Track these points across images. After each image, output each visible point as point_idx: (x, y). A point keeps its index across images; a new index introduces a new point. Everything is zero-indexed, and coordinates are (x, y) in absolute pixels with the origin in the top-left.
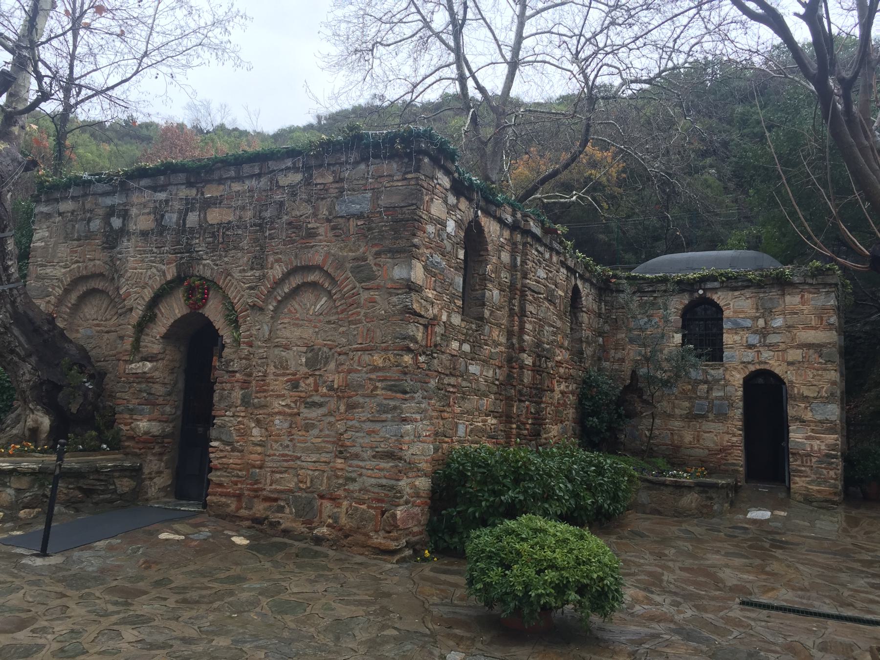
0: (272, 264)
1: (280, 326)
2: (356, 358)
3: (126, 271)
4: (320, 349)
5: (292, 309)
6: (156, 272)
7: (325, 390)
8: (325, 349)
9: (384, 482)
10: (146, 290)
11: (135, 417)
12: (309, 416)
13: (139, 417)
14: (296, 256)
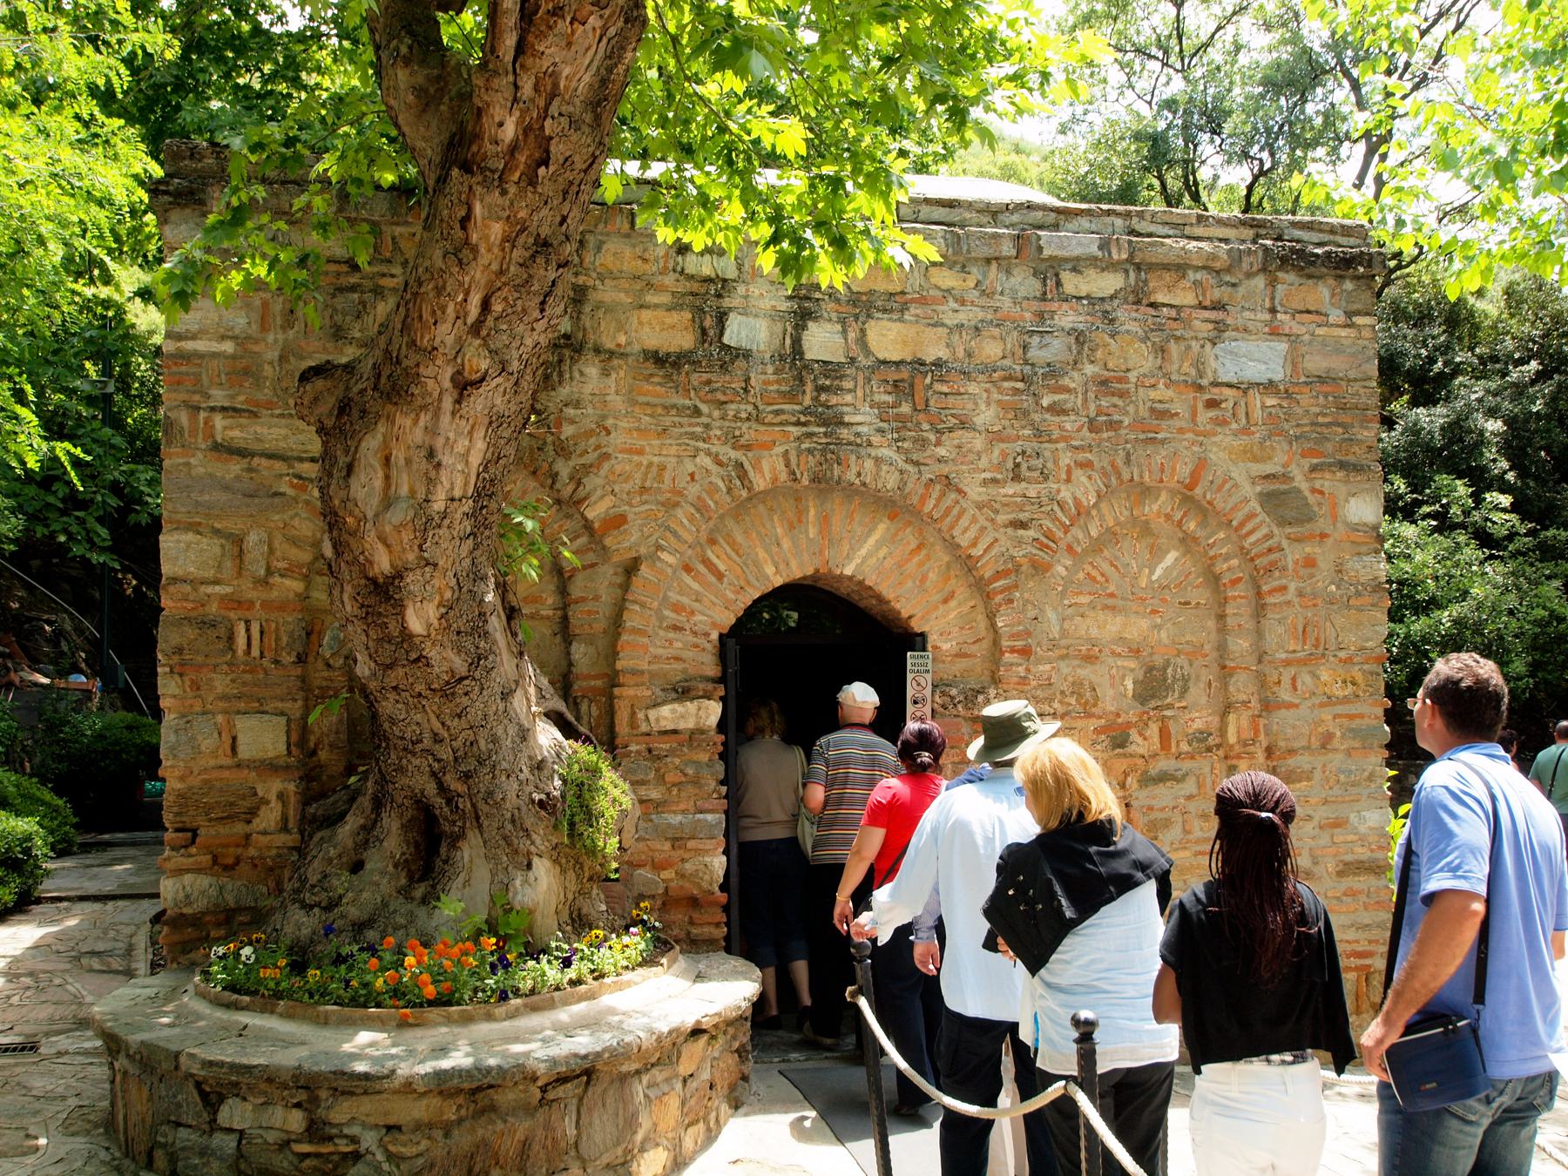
0: (1069, 472)
1: (1070, 611)
2: (1286, 680)
3: (606, 456)
4: (1167, 664)
5: (1094, 573)
6: (714, 468)
7: (1185, 747)
8: (1182, 661)
9: (1366, 918)
10: (679, 513)
11: (691, 844)
12: (1157, 803)
13: (709, 844)
14: (1128, 461)
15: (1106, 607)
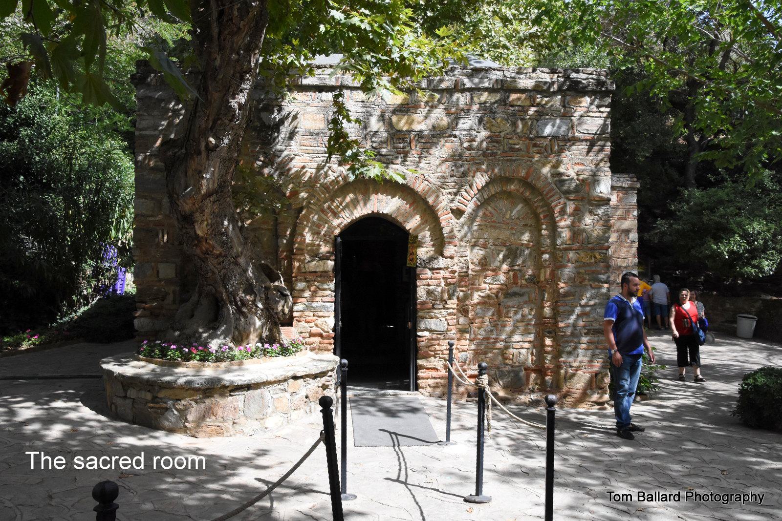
4: (517, 249)
7: (524, 282)
15: (491, 226)
